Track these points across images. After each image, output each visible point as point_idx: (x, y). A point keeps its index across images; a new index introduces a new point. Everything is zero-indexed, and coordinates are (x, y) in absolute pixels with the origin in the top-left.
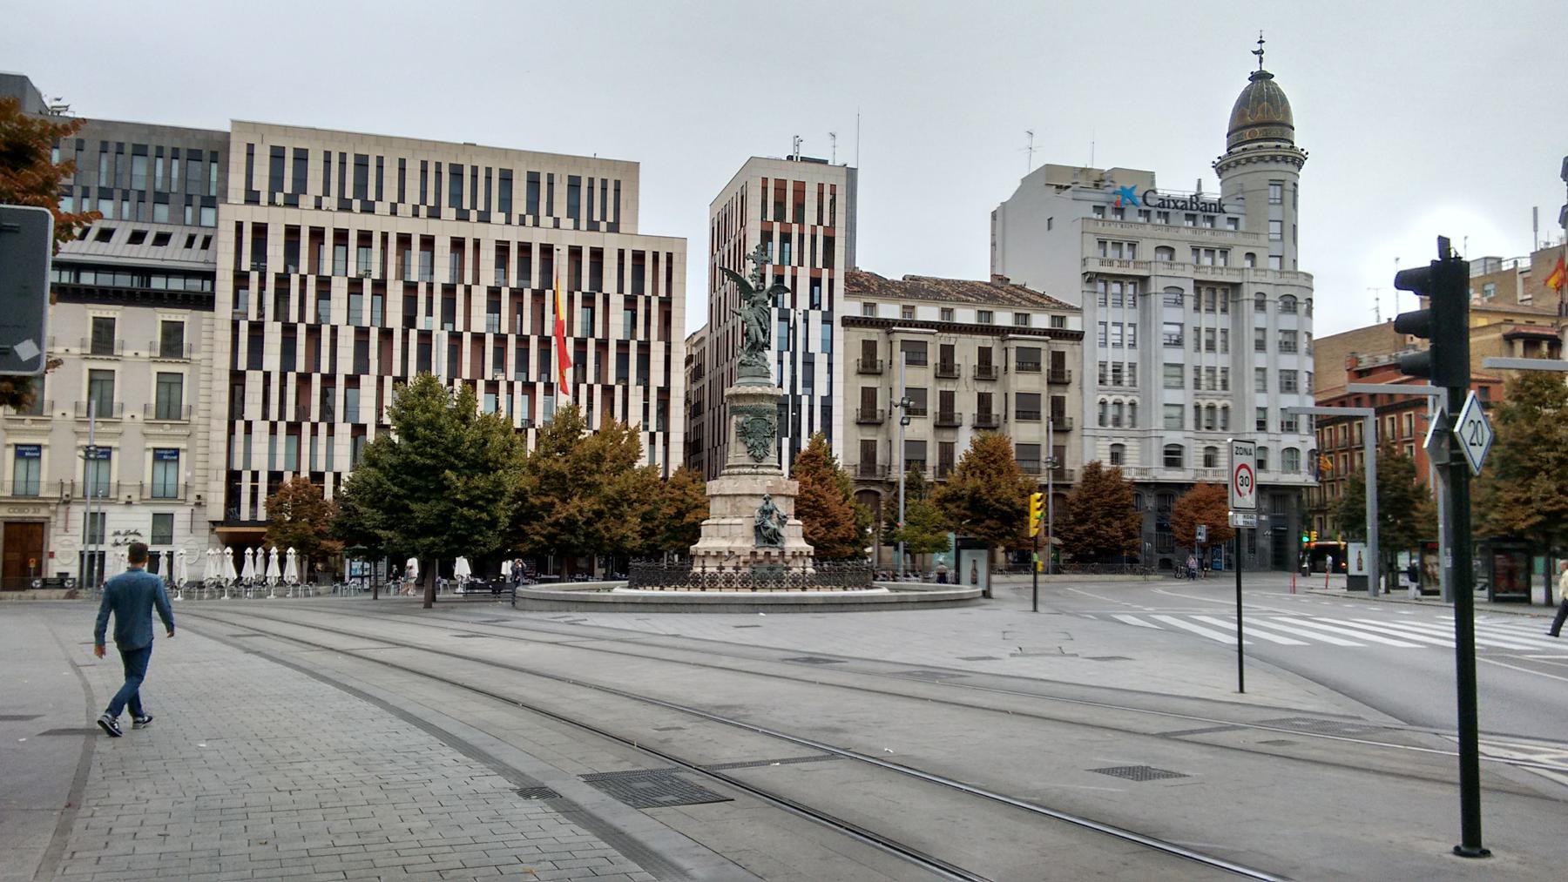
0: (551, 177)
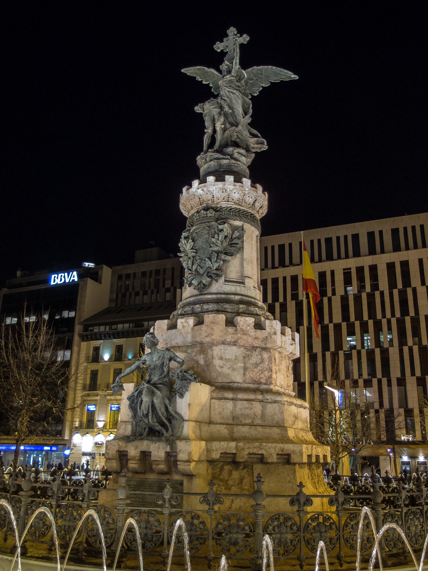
0: (381, 232)
